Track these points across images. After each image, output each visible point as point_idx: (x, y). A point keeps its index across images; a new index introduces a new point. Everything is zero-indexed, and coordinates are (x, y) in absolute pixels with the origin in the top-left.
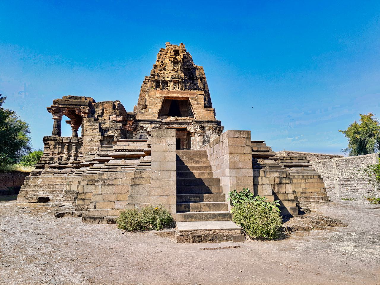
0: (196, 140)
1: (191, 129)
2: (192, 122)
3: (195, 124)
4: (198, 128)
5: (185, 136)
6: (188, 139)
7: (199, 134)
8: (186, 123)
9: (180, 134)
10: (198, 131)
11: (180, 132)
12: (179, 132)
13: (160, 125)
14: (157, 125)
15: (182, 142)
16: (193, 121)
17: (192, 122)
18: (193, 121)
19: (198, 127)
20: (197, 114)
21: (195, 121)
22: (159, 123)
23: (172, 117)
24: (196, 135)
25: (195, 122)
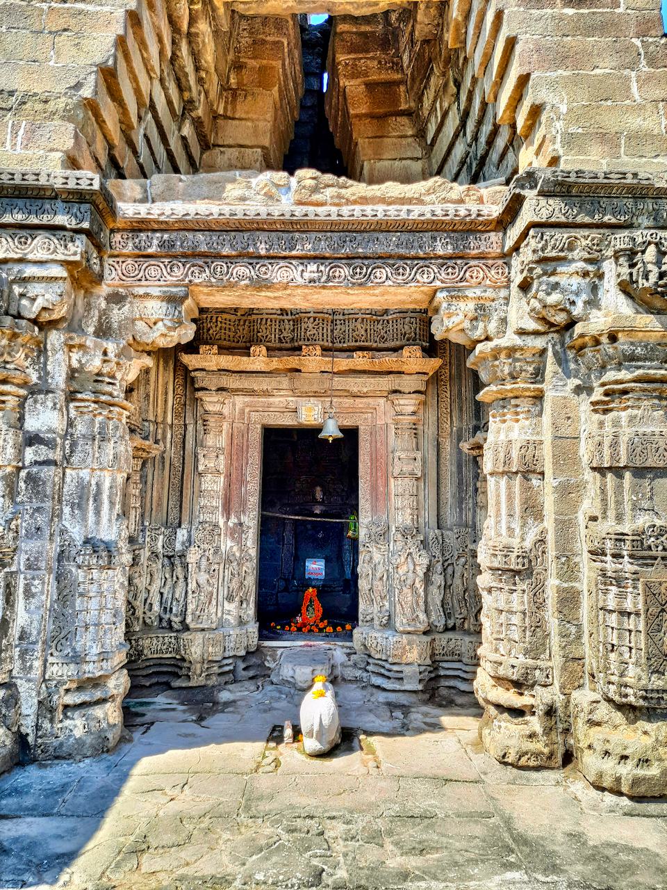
0: (565, 444)
1: (491, 312)
2: (514, 206)
3: (562, 236)
4: (609, 286)
5: (408, 404)
6: (431, 431)
7: (611, 375)
8: (435, 228)
9: (355, 384)
10: (597, 322)
11: (360, 361)
12: (343, 363)
13: (76, 249)
14: (39, 247)
15: (374, 459)
16: (530, 194)
17: (514, 206)
18: (530, 194)
19: (608, 267)
20: (574, 116)
21: (561, 189)
22: (61, 219)
23: (254, 181)
24: (557, 388)
25: (553, 209)
